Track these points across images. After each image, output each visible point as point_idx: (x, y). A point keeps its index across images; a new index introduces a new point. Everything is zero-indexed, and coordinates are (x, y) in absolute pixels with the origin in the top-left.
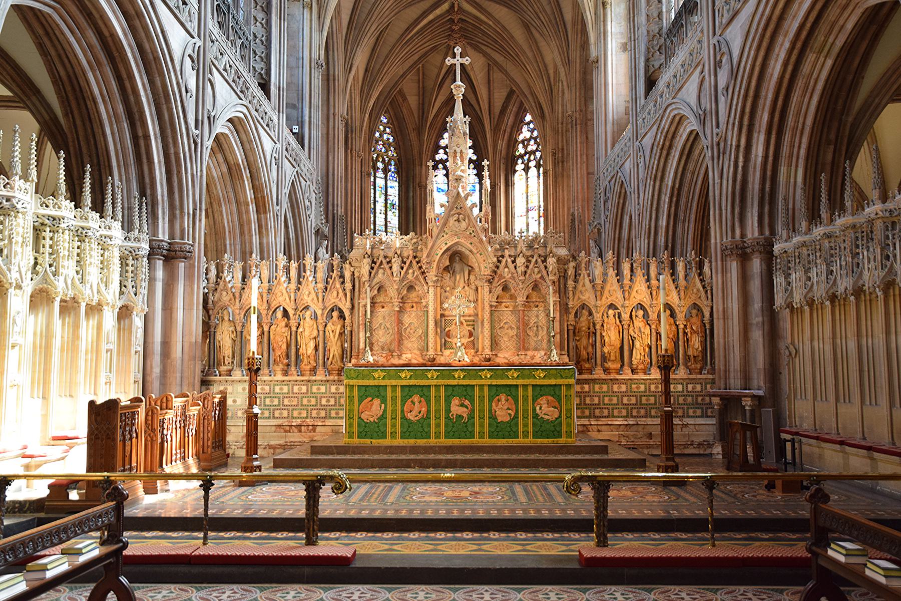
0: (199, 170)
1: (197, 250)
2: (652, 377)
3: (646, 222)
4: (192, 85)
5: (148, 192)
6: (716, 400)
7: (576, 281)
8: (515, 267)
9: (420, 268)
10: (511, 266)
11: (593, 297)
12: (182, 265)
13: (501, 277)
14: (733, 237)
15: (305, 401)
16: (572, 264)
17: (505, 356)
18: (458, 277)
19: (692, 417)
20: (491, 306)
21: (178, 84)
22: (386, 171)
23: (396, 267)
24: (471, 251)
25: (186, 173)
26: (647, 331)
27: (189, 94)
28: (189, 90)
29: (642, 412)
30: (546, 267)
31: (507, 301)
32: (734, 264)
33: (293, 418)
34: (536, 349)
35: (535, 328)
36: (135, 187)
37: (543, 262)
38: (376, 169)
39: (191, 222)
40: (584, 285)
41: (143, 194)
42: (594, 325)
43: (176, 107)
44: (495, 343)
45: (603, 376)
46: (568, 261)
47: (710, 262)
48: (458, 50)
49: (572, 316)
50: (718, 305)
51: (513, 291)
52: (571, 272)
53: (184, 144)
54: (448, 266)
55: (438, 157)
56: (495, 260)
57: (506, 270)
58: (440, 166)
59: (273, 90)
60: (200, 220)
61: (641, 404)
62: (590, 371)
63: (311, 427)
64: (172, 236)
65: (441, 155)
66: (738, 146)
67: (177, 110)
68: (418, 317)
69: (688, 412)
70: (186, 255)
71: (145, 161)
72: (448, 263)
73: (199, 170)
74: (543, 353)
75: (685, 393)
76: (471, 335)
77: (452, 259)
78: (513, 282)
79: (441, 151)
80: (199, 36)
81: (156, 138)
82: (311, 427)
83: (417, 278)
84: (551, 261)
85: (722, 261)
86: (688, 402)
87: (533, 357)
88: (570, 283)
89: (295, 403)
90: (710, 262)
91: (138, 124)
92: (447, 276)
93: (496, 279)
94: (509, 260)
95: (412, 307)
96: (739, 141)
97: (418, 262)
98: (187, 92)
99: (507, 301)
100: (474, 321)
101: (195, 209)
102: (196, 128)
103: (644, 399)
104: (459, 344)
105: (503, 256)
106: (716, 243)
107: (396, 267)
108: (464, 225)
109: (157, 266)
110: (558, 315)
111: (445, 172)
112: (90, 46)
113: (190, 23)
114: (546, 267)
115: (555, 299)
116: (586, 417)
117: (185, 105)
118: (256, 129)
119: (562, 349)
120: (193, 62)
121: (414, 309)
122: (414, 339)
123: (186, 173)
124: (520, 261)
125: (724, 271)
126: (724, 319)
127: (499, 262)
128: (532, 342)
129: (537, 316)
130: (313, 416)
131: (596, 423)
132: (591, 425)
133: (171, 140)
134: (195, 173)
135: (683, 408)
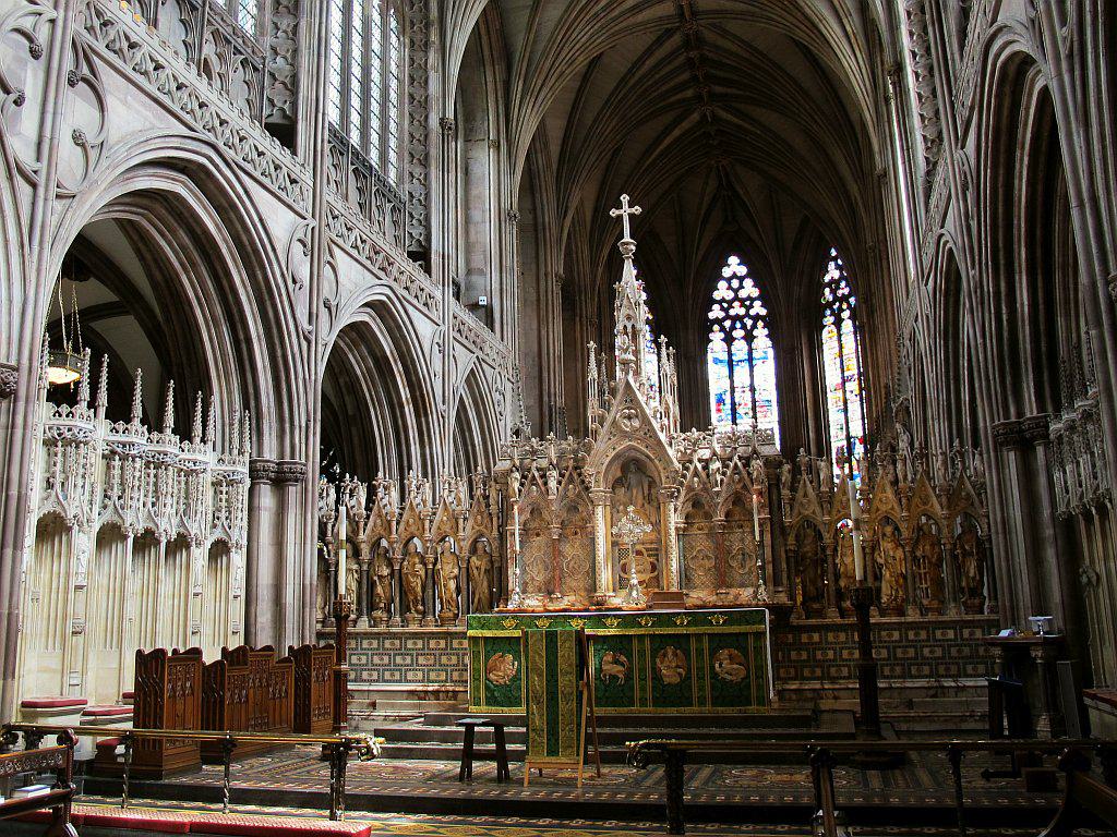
0: (313, 372)
1: (310, 471)
2: (910, 619)
4: (304, 273)
5: (252, 403)
6: (997, 651)
7: (793, 489)
8: (708, 475)
9: (583, 482)
10: (703, 475)
11: (818, 510)
12: (292, 489)
14: (1007, 415)
15: (444, 660)
16: (787, 467)
17: (699, 595)
18: (635, 492)
19: (971, 676)
20: (677, 529)
21: (283, 275)
23: (553, 484)
24: (648, 456)
25: (296, 378)
26: (899, 553)
27: (298, 285)
28: (298, 279)
29: (898, 670)
30: (749, 474)
31: (699, 522)
32: (1012, 455)
33: (429, 681)
34: (743, 585)
35: (740, 557)
36: (237, 400)
37: (745, 466)
39: (303, 437)
40: (805, 495)
41: (246, 406)
42: (824, 549)
43: (282, 302)
44: (686, 578)
45: (838, 620)
46: (780, 465)
47: (981, 454)
48: (625, 198)
49: (791, 540)
50: (995, 515)
51: (707, 508)
52: (786, 477)
53: (293, 343)
54: (620, 478)
55: (711, 315)
57: (696, 479)
58: (716, 327)
60: (314, 434)
61: (896, 659)
62: (820, 613)
63: (451, 694)
64: (281, 454)
65: (716, 312)
67: (283, 305)
68: (583, 546)
69: (964, 668)
70: (299, 478)
71: (248, 367)
72: (619, 474)
73: (313, 372)
74: (751, 590)
75: (959, 642)
76: (654, 568)
77: (625, 468)
78: (705, 495)
79: (716, 307)
80: (313, 216)
81: (259, 339)
82: (451, 694)
83: (579, 495)
84: (757, 464)
85: (995, 451)
86: (964, 654)
87: (737, 597)
88: (785, 492)
89: (432, 662)
90: (981, 454)
91: (239, 326)
93: (683, 493)
94: (699, 466)
95: (576, 533)
97: (580, 475)
98: (294, 282)
99: (699, 522)
100: (657, 550)
101: (308, 420)
102: (310, 323)
103: (899, 651)
104: (634, 581)
105: (691, 462)
106: (986, 427)
108: (636, 423)
109: (262, 491)
110: (768, 538)
111: (722, 335)
112: (183, 247)
113: (302, 203)
114: (749, 474)
115: (762, 516)
116: (818, 678)
117: (293, 299)
118: (406, 312)
119: (777, 582)
120: (305, 246)
121: (579, 536)
122: (580, 576)
123: (296, 378)
125: (1000, 466)
126: (1005, 533)
128: (738, 573)
129: (742, 540)
130: (454, 679)
131: (830, 686)
132: (824, 689)
133: (277, 341)
134: (307, 377)
135: (958, 664)
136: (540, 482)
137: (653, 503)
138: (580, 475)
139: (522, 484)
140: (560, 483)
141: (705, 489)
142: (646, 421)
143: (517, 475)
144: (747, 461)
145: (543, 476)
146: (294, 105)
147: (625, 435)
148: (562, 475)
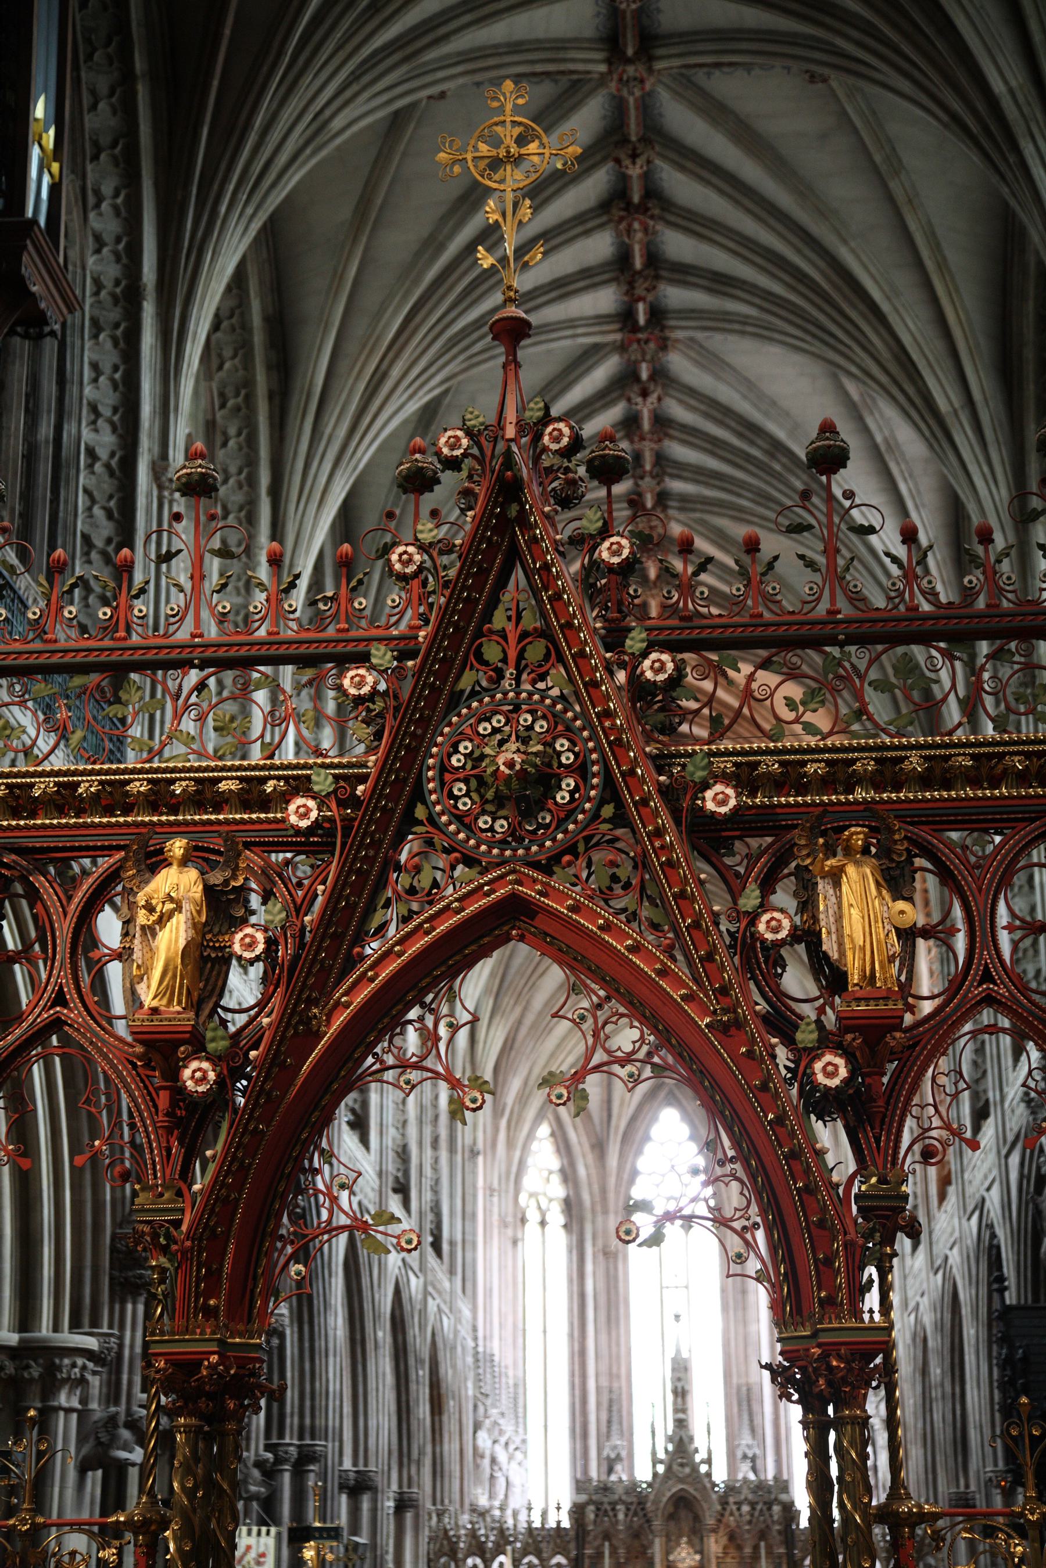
3: (920, 1425)
9: (645, 1515)
10: (737, 1513)
13: (727, 1526)
14: (958, 1487)
22: (543, 1223)
23: (621, 1516)
38: (523, 1220)
56: (719, 1508)
59: (445, 1247)
66: (953, 1394)
92: (672, 1524)
94: (734, 1507)
96: (953, 1389)
99: (732, 1551)
105: (727, 1503)
107: (621, 1516)
108: (687, 1470)
124: (746, 1508)
127: (724, 1509)
136: (611, 1514)
137: (697, 1535)
138: (643, 1509)
139: (597, 1516)
140: (626, 1515)
141: (738, 1527)
142: (695, 1468)
143: (592, 1508)
144: (769, 1505)
145: (613, 1509)
146: (406, 1173)
147: (681, 1480)
148: (628, 1509)
